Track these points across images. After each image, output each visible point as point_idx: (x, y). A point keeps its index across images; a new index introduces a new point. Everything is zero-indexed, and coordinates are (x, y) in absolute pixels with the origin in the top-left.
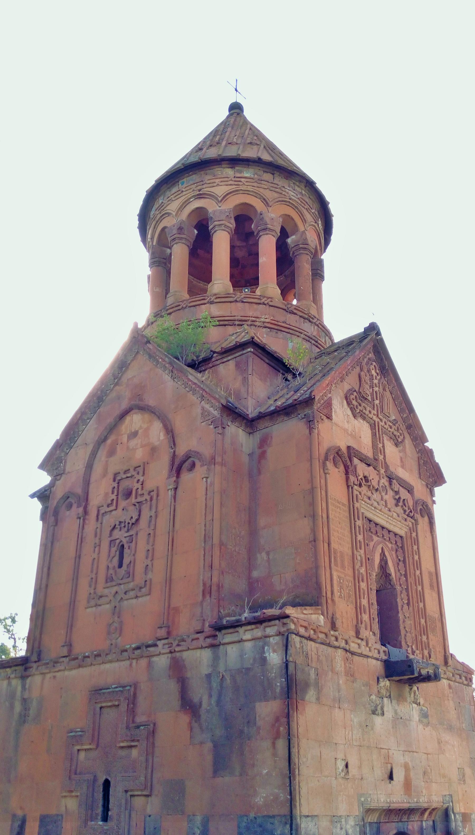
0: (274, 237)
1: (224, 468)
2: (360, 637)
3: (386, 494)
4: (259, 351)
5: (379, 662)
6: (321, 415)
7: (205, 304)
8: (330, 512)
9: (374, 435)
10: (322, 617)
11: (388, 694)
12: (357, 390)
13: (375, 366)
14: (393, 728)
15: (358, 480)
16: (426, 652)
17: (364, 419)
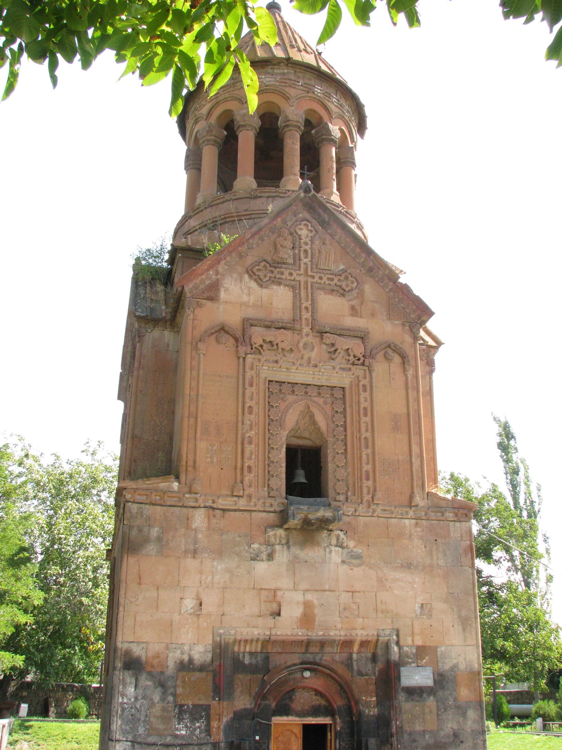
0: (248, 130)
1: (141, 372)
2: (234, 494)
3: (312, 350)
4: (191, 253)
5: (272, 514)
6: (198, 300)
7: (187, 220)
8: (200, 388)
9: (296, 297)
10: (177, 484)
11: (284, 542)
12: (269, 259)
13: (305, 225)
14: (287, 570)
15: (252, 349)
16: (367, 497)
17: (280, 284)
